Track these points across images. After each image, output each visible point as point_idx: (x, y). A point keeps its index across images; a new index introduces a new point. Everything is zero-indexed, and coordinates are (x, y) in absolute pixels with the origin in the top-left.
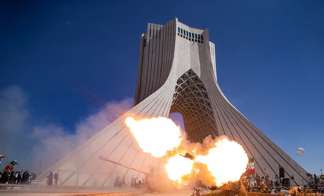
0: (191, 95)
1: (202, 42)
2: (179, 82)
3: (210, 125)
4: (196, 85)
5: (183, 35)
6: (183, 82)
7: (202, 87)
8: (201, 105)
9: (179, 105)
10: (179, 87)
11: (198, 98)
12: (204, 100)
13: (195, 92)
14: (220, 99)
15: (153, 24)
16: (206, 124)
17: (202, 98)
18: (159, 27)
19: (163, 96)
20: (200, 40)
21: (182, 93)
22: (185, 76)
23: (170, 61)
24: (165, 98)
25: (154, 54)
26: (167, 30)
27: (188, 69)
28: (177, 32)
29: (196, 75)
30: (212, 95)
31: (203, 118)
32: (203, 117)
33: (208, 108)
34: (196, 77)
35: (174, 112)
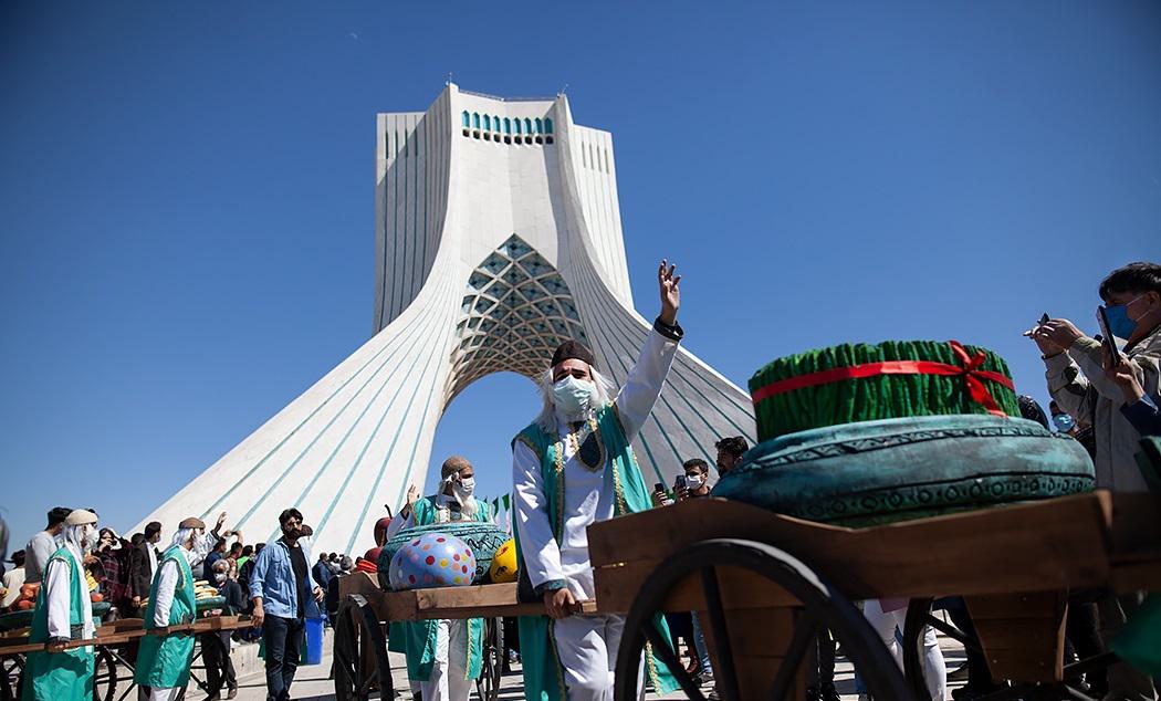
0: (529, 313)
1: (549, 141)
2: (476, 280)
4: (539, 280)
7: (558, 284)
11: (551, 320)
14: (612, 314)
15: (391, 116)
18: (411, 120)
19: (414, 337)
22: (496, 260)
24: (421, 342)
25: (401, 208)
29: (532, 249)
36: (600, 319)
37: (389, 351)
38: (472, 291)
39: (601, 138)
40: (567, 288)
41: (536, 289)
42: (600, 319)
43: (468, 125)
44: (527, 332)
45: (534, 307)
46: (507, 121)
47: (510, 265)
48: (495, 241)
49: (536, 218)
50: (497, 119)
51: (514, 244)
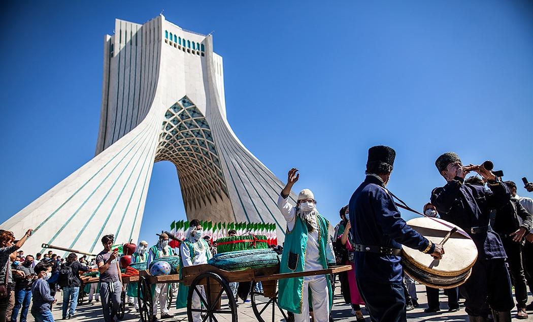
0: (187, 134)
3: (215, 178)
4: (195, 120)
5: (173, 42)
6: (174, 115)
7: (203, 123)
8: (202, 149)
9: (168, 150)
10: (169, 124)
11: (198, 139)
14: (229, 140)
15: (124, 22)
16: (211, 177)
17: (203, 139)
18: (135, 27)
19: (143, 139)
20: (202, 50)
21: (174, 132)
23: (153, 84)
25: (127, 70)
26: (148, 33)
28: (164, 38)
30: (218, 136)
31: (205, 169)
32: (206, 167)
33: (213, 154)
34: (193, 107)
36: (223, 142)
37: (133, 143)
38: (165, 119)
39: (218, 58)
40: (208, 126)
41: (193, 123)
42: (223, 142)
43: (167, 38)
44: (184, 144)
46: (184, 41)
47: (182, 110)
48: (177, 98)
49: (196, 90)
50: (180, 38)
51: (185, 100)
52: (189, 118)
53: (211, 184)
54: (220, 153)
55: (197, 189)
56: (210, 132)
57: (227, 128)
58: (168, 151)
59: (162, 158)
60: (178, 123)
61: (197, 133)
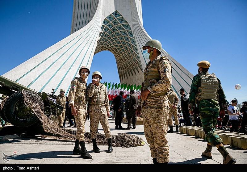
0: (118, 34)
4: (122, 25)
7: (128, 26)
8: (126, 42)
9: (107, 43)
12: (129, 38)
13: (122, 31)
16: (132, 59)
19: (88, 33)
21: (110, 33)
24: (90, 35)
27: (114, 11)
30: (136, 33)
31: (129, 55)
32: (129, 53)
33: (133, 44)
34: (121, 17)
35: (104, 50)
40: (130, 28)
45: (120, 32)
52: (119, 24)
53: (132, 64)
54: (137, 44)
55: (125, 68)
56: (132, 31)
57: (141, 29)
58: (107, 44)
59: (104, 49)
60: (113, 27)
61: (124, 33)
